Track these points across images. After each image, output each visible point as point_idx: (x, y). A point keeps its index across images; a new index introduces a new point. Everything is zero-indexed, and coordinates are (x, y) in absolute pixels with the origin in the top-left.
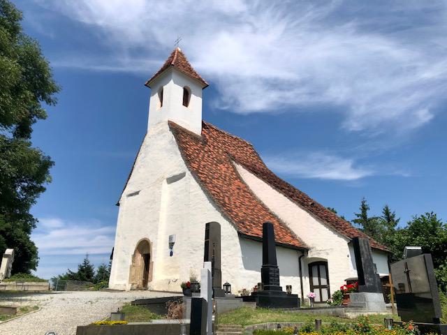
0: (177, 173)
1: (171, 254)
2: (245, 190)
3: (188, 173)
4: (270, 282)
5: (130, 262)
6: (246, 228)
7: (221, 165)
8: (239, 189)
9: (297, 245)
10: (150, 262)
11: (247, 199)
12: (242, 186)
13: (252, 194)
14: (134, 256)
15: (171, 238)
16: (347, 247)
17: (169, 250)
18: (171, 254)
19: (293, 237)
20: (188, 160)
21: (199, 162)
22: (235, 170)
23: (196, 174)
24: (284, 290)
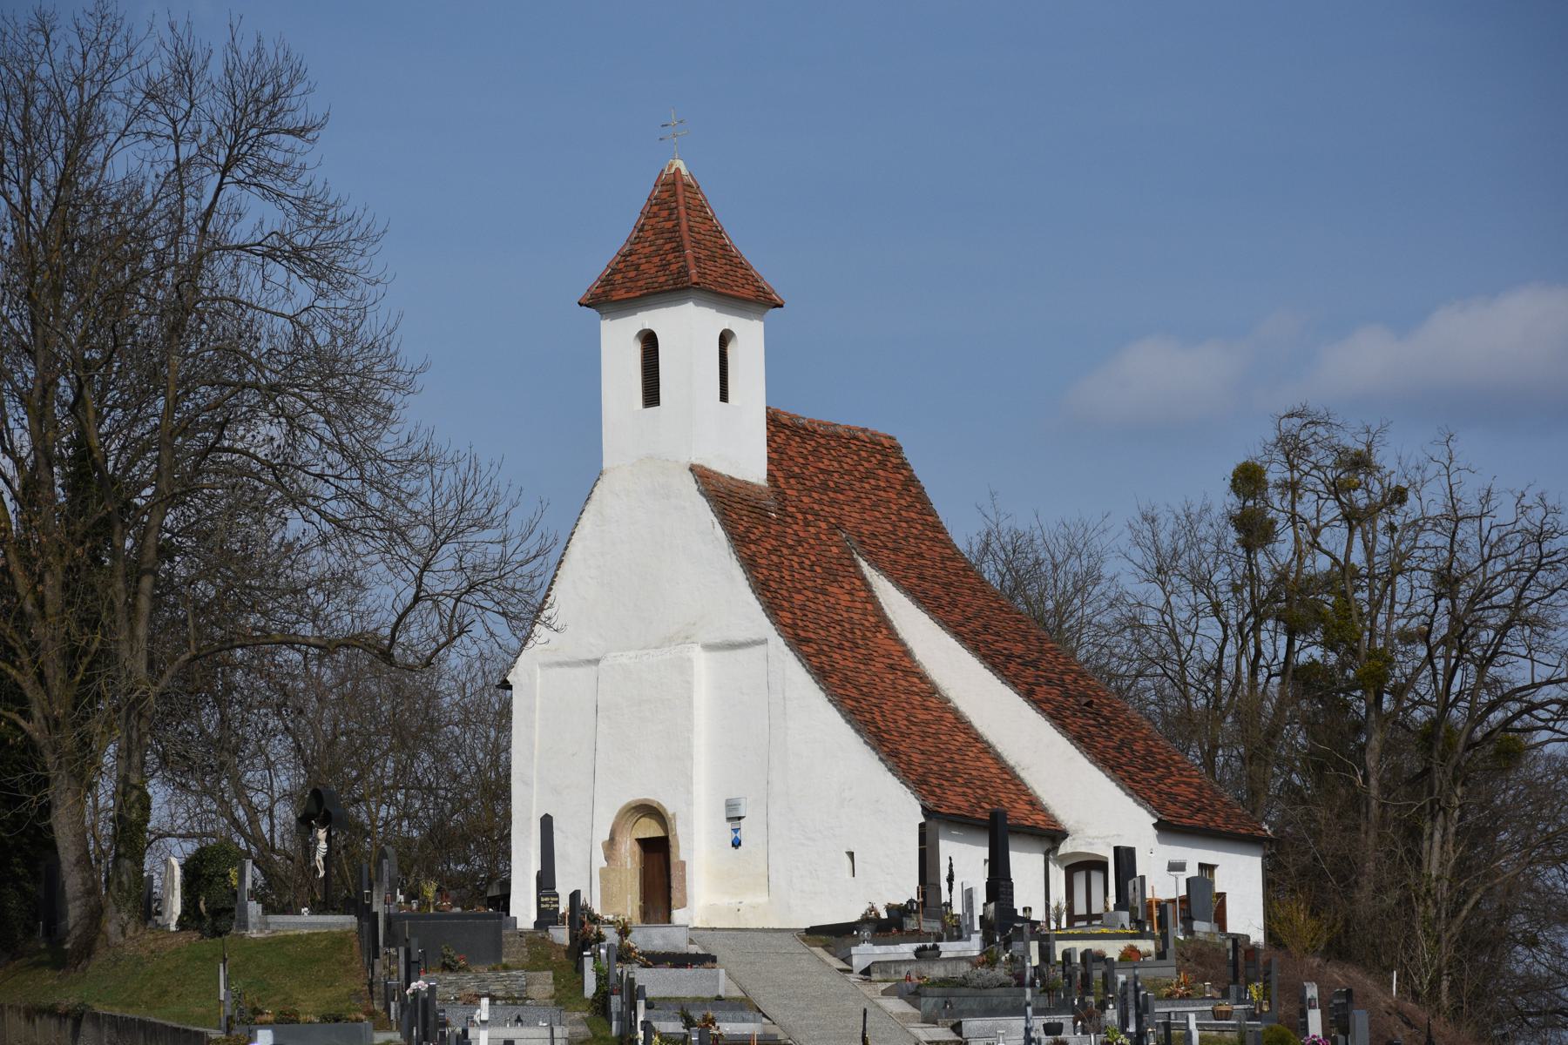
0: (740, 636)
1: (736, 844)
2: (904, 665)
3: (777, 644)
4: (1002, 896)
5: (600, 861)
6: (932, 793)
7: (833, 589)
8: (892, 667)
9: (1042, 825)
10: (673, 859)
11: (916, 700)
12: (894, 648)
13: (923, 678)
14: (611, 845)
15: (731, 805)
16: (1154, 832)
17: (729, 837)
18: (736, 844)
19: (1034, 803)
20: (772, 609)
21: (789, 600)
22: (871, 598)
23: (797, 641)
24: (1020, 913)
